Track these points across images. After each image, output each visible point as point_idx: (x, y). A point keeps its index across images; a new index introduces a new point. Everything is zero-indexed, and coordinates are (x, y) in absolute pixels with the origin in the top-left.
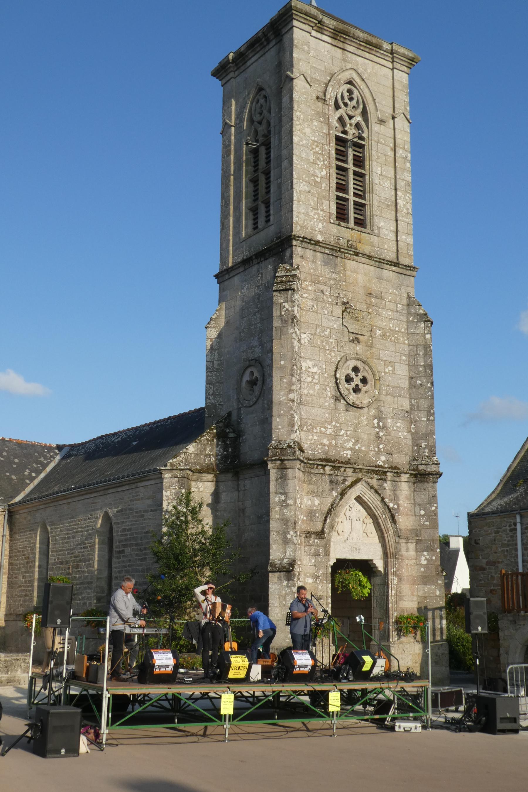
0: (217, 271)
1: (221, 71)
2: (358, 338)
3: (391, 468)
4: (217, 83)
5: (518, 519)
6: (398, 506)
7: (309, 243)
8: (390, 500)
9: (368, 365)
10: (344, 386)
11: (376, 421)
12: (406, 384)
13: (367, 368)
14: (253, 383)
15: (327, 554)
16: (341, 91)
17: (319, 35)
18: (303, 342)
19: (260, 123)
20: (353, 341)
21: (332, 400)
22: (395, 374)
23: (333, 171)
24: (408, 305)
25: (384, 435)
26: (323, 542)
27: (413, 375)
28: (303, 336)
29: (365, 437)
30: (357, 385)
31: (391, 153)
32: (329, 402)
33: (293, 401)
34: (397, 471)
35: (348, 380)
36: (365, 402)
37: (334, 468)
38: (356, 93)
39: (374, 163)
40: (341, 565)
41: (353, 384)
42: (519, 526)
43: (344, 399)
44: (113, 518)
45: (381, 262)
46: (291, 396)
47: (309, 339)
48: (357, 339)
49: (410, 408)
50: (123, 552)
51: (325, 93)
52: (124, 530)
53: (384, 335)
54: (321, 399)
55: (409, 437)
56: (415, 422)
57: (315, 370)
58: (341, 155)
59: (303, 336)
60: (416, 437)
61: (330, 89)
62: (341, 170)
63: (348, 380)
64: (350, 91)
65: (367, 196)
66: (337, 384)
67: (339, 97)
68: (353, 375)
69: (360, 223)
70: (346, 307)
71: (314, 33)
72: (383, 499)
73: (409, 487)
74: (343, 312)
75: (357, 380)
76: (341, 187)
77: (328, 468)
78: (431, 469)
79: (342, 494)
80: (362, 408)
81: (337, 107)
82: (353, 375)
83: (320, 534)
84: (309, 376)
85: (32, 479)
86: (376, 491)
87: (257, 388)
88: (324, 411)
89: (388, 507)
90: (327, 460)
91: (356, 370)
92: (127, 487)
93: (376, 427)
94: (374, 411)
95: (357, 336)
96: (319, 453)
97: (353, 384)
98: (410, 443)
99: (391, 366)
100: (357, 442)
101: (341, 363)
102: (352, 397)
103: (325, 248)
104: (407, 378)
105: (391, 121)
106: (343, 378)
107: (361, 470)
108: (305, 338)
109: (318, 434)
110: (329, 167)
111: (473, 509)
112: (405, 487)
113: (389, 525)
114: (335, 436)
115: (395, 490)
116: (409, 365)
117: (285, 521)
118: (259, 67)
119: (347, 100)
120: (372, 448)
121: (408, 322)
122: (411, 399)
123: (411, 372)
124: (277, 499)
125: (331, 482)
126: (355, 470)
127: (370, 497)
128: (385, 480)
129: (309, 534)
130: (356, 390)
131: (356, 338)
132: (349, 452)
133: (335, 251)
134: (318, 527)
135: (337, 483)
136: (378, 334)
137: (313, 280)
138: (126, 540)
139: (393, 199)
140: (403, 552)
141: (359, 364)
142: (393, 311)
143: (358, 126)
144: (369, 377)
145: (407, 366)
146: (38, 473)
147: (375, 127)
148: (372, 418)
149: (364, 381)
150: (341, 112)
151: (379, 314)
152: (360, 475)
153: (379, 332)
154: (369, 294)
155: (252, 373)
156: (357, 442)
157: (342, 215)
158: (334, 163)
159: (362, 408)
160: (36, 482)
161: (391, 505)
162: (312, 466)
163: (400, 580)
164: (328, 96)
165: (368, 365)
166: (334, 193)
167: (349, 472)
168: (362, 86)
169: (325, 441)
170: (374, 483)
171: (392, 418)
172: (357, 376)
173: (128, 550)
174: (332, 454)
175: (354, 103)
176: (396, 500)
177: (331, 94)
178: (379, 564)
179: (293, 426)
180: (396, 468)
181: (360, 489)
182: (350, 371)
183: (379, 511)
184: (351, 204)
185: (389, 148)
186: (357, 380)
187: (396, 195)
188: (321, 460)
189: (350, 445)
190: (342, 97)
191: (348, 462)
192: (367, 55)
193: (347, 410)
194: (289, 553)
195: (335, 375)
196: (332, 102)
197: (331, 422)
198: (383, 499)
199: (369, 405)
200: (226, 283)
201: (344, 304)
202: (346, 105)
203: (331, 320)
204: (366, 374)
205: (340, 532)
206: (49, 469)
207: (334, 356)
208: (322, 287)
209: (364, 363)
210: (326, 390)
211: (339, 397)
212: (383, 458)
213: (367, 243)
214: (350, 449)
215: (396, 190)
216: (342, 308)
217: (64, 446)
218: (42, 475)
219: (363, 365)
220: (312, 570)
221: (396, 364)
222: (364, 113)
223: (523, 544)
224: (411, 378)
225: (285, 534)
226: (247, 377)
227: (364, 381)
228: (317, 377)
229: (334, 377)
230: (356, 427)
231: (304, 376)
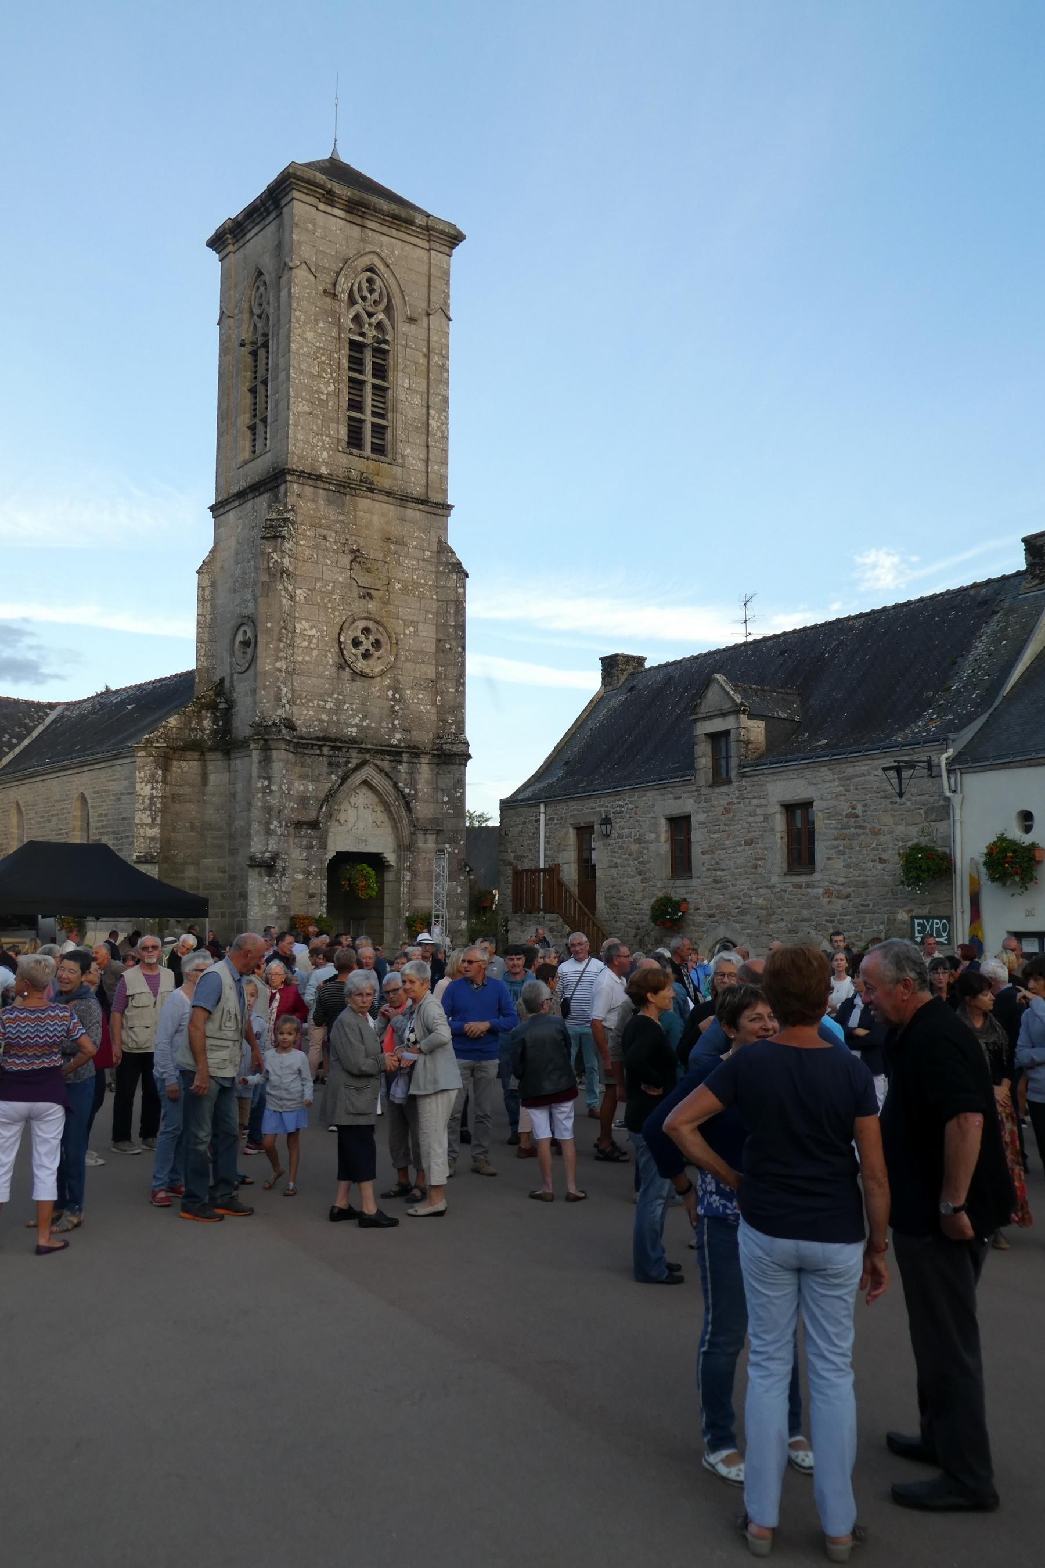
3: (409, 747)
4: (213, 256)
5: (542, 810)
6: (416, 791)
8: (406, 785)
9: (382, 626)
10: (350, 652)
11: (390, 693)
12: (431, 647)
13: (381, 629)
14: (246, 644)
15: (324, 846)
16: (358, 280)
17: (329, 209)
18: (298, 599)
19: (260, 317)
20: (364, 597)
21: (334, 669)
23: (344, 387)
24: (438, 552)
25: (401, 709)
26: (318, 833)
28: (298, 592)
29: (377, 711)
30: (367, 650)
31: (422, 361)
32: (330, 671)
33: (280, 671)
34: (415, 752)
35: (356, 643)
36: (377, 670)
37: (333, 748)
38: (378, 283)
39: (400, 374)
40: (342, 858)
41: (362, 649)
42: (542, 815)
43: (349, 666)
44: (89, 801)
45: (403, 499)
46: (278, 665)
48: (369, 594)
51: (335, 285)
52: (100, 815)
53: (405, 589)
55: (434, 710)
57: (313, 632)
58: (356, 363)
59: (298, 592)
60: (442, 712)
61: (342, 279)
62: (356, 385)
63: (356, 643)
64: (370, 281)
65: (390, 415)
66: (341, 649)
67: (355, 288)
68: (362, 638)
69: (379, 449)
70: (356, 556)
71: (322, 206)
72: (395, 785)
73: (431, 770)
74: (352, 562)
75: (367, 644)
76: (355, 405)
77: (326, 751)
78: (456, 749)
79: (344, 779)
80: (373, 677)
81: (352, 302)
82: (362, 638)
83: (314, 825)
85: (12, 747)
86: (387, 775)
89: (402, 792)
90: (326, 739)
91: (366, 631)
92: (103, 765)
93: (391, 700)
95: (371, 591)
96: (315, 730)
97: (362, 649)
98: (434, 717)
100: (365, 717)
101: (347, 624)
102: (361, 665)
103: (330, 483)
105: (425, 319)
106: (349, 642)
107: (368, 750)
110: (337, 381)
111: (507, 794)
112: (425, 770)
113: (403, 812)
114: (337, 710)
115: (412, 773)
116: (437, 625)
117: (268, 809)
118: (259, 242)
119: (366, 293)
120: (384, 724)
121: (437, 572)
122: (437, 665)
124: (259, 785)
125: (330, 764)
126: (361, 751)
127: (379, 780)
128: (400, 762)
129: (299, 825)
130: (366, 655)
132: (355, 730)
133: (343, 487)
134: (312, 815)
135: (338, 765)
138: (103, 827)
139: (424, 419)
140: (420, 844)
141: (370, 624)
143: (380, 326)
144: (384, 639)
146: (21, 738)
147: (404, 328)
149: (377, 644)
150: (358, 308)
151: (399, 563)
152: (367, 756)
153: (398, 586)
155: (245, 631)
156: (365, 717)
157: (355, 439)
158: (346, 374)
159: (373, 677)
160: (17, 750)
161: (407, 790)
162: (306, 746)
163: (414, 875)
164: (339, 289)
165: (382, 626)
166: (344, 413)
167: (354, 754)
168: (387, 274)
169: (324, 717)
170: (386, 765)
171: (412, 688)
172: (368, 639)
174: (333, 731)
176: (413, 784)
177: (343, 285)
178: (391, 857)
179: (279, 700)
180: (415, 747)
181: (367, 772)
182: (359, 634)
183: (391, 797)
184: (368, 427)
185: (421, 354)
186: (367, 644)
187: (428, 414)
188: (318, 739)
189: (357, 720)
190: (360, 289)
191: (353, 741)
192: (394, 233)
194: (273, 845)
196: (345, 297)
197: (333, 693)
198: (395, 785)
199: (382, 674)
200: (222, 518)
201: (352, 551)
202: (364, 298)
203: (335, 572)
204: (379, 637)
205: (342, 821)
206: (35, 734)
208: (324, 532)
209: (378, 623)
210: (326, 656)
211: (343, 664)
212: (398, 736)
213: (388, 476)
214: (356, 725)
215: (428, 407)
216: (350, 557)
217: (58, 704)
218: (26, 742)
219: (375, 625)
220: (303, 865)
223: (545, 837)
224: (439, 641)
225: (268, 824)
226: (240, 638)
228: (315, 641)
230: (364, 700)
231: (298, 640)
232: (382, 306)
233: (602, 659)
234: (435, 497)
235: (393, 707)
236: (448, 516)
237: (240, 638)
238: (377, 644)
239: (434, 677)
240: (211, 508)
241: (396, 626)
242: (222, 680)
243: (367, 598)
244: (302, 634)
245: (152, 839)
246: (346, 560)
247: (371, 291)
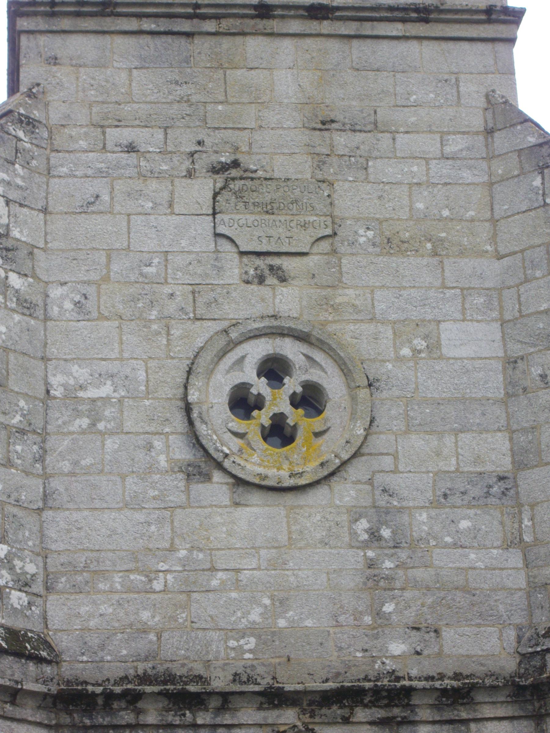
2: (279, 268)
9: (321, 345)
13: (319, 356)
18: (55, 311)
20: (261, 280)
22: (441, 357)
25: (401, 566)
27: (516, 350)
43: (219, 466)
47: (77, 298)
49: (513, 462)
54: (130, 480)
55: (515, 559)
56: (532, 506)
57: (106, 390)
63: (243, 403)
84: (78, 414)
88: (140, 516)
91: (274, 370)
93: (365, 545)
94: (352, 493)
95: (276, 261)
99: (426, 337)
101: (207, 357)
103: (139, 16)
104: (498, 366)
108: (63, 297)
109: (116, 597)
116: (503, 323)
123: (510, 345)
130: (279, 433)
131: (271, 268)
132: (251, 642)
136: (362, 240)
137: (96, 119)
141: (290, 349)
142: (427, 160)
144: (333, 384)
145: (496, 325)
148: (345, 517)
154: (323, 123)
165: (321, 345)
171: (435, 504)
186: (278, 401)
193: (237, 504)
195: (186, 395)
197: (172, 549)
201: (218, 169)
204: (315, 376)
207: (181, 338)
208: (126, 135)
209: (302, 337)
210: (149, 447)
211: (205, 463)
214: (252, 630)
219: (304, 348)
221: (443, 326)
224: (511, 362)
227: (310, 399)
229: (181, 404)
231: (58, 417)
235: (371, 564)
236: (512, 41)
239: (506, 464)
241: (356, 336)
243: (271, 280)
244: (71, 396)
246: (203, 188)
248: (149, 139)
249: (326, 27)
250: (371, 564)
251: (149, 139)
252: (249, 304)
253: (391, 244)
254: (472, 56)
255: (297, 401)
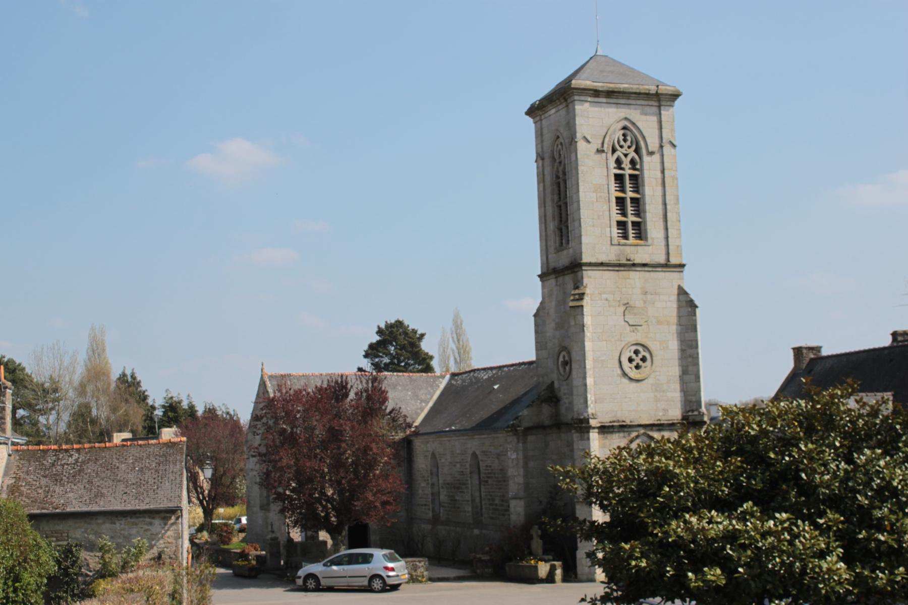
0: (540, 273)
1: (534, 111)
4: (530, 120)
7: (636, 180)
14: (565, 363)
17: (596, 100)
41: (634, 363)
50: (487, 482)
63: (631, 360)
64: (624, 135)
68: (634, 356)
81: (614, 150)
87: (567, 368)
91: (636, 352)
97: (634, 363)
102: (633, 373)
119: (622, 143)
130: (637, 367)
141: (640, 349)
147: (646, 159)
150: (619, 153)
173: (490, 481)
175: (629, 143)
186: (637, 360)
190: (619, 142)
202: (621, 147)
203: (616, 319)
216: (622, 308)
222: (637, 151)
226: (561, 359)
232: (634, 147)
233: (794, 349)
234: (674, 260)
237: (561, 359)
238: (644, 359)
240: (539, 276)
242: (553, 383)
245: (519, 484)
247: (625, 140)
248: (610, 297)
249: (646, 269)
250: (656, 396)
251: (610, 297)
252: (634, 338)
253: (659, 323)
254: (676, 275)
255: (642, 360)
